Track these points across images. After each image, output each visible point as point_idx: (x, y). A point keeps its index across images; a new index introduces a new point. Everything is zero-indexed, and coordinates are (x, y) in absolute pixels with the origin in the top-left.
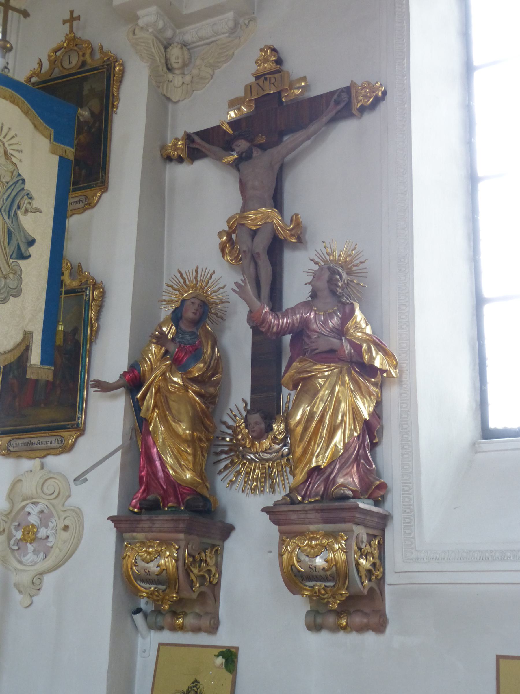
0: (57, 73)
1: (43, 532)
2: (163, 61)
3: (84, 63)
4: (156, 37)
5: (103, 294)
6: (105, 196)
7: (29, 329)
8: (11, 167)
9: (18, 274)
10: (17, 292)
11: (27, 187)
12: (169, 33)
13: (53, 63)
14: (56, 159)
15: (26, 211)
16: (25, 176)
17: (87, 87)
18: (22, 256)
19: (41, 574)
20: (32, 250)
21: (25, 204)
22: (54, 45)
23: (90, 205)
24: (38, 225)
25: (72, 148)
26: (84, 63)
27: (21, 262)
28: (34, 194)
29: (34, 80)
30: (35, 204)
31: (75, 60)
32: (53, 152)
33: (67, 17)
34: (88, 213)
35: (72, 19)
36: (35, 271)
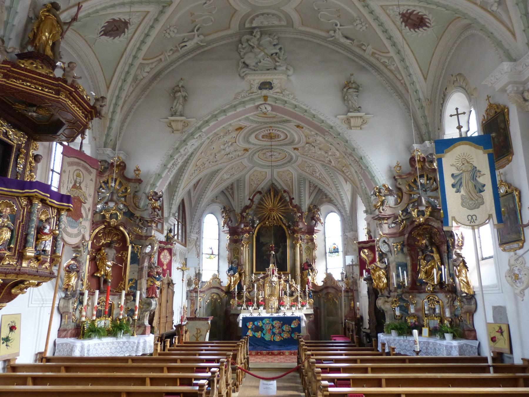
0: (489, 117)
1: (520, 276)
2: (522, 100)
3: (496, 112)
4: (516, 93)
5: (520, 193)
6: (514, 156)
7: (490, 213)
8: (470, 165)
9: (482, 198)
10: (483, 203)
11: (477, 169)
12: (521, 89)
13: (487, 114)
14: (486, 155)
15: (479, 177)
16: (475, 166)
17: (499, 120)
18: (481, 191)
19: (523, 290)
20: (485, 188)
21: (478, 175)
22: (485, 109)
23: (510, 161)
24: (486, 179)
25: (491, 148)
26: (496, 112)
27: (482, 193)
28: (481, 170)
29: (484, 122)
30: (482, 173)
31: (493, 111)
32: (484, 153)
33: (487, 98)
34: (510, 164)
35: (488, 97)
36: (488, 195)
